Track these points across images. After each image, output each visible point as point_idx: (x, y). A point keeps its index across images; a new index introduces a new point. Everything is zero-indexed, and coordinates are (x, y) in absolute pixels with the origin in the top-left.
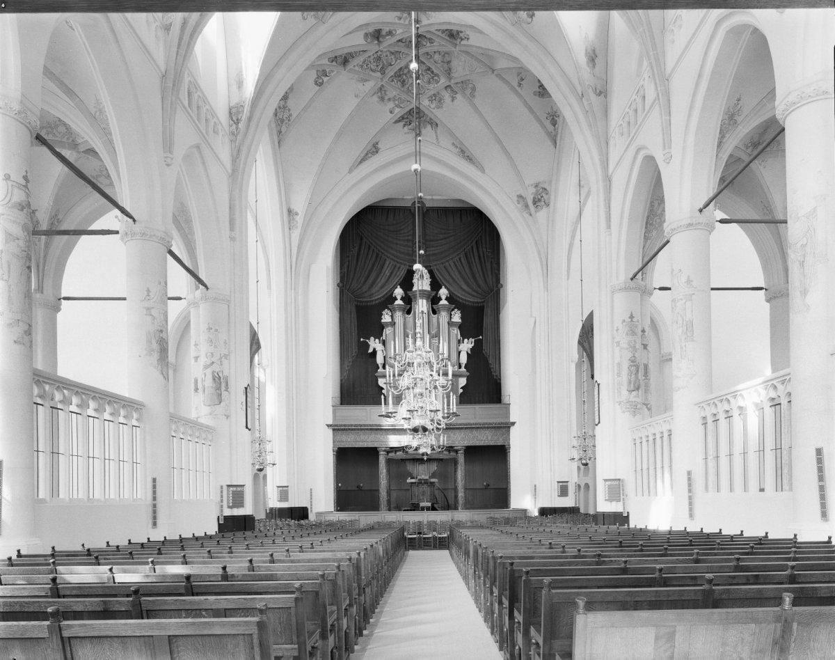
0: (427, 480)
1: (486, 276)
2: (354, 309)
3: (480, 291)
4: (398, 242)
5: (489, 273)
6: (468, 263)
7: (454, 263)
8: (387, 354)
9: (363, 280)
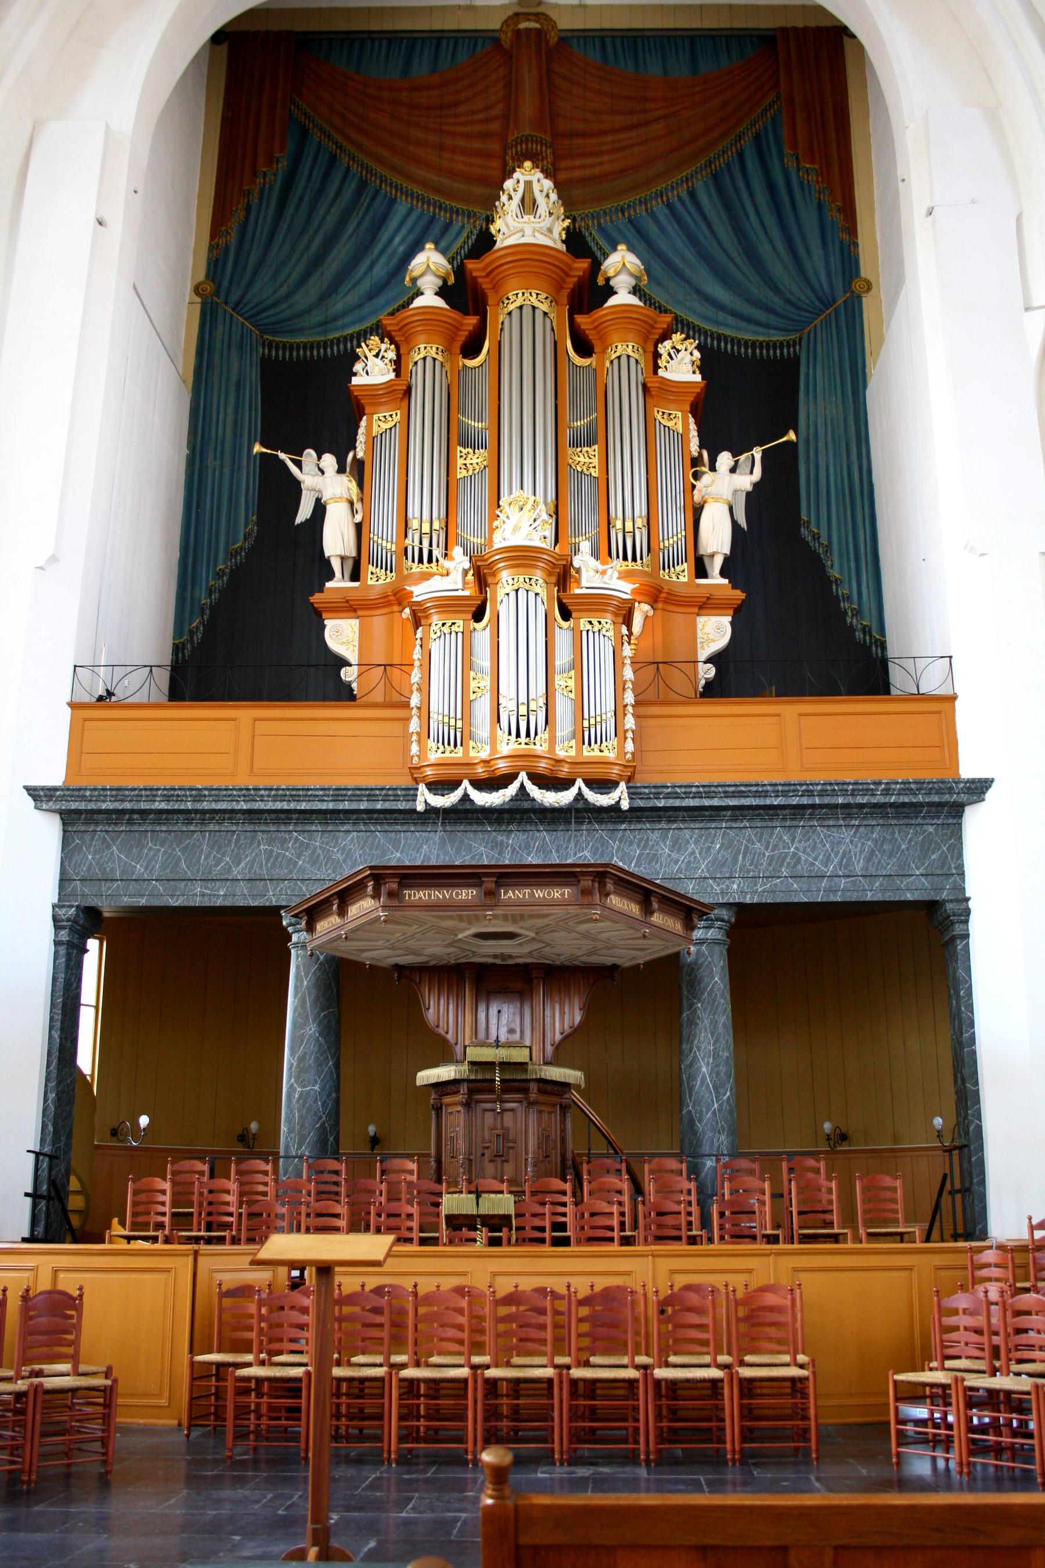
0: (521, 1066)
1: (802, 252)
2: (253, 375)
3: (776, 302)
4: (449, 141)
5: (815, 242)
6: (727, 206)
7: (670, 206)
8: (368, 514)
9: (300, 269)
